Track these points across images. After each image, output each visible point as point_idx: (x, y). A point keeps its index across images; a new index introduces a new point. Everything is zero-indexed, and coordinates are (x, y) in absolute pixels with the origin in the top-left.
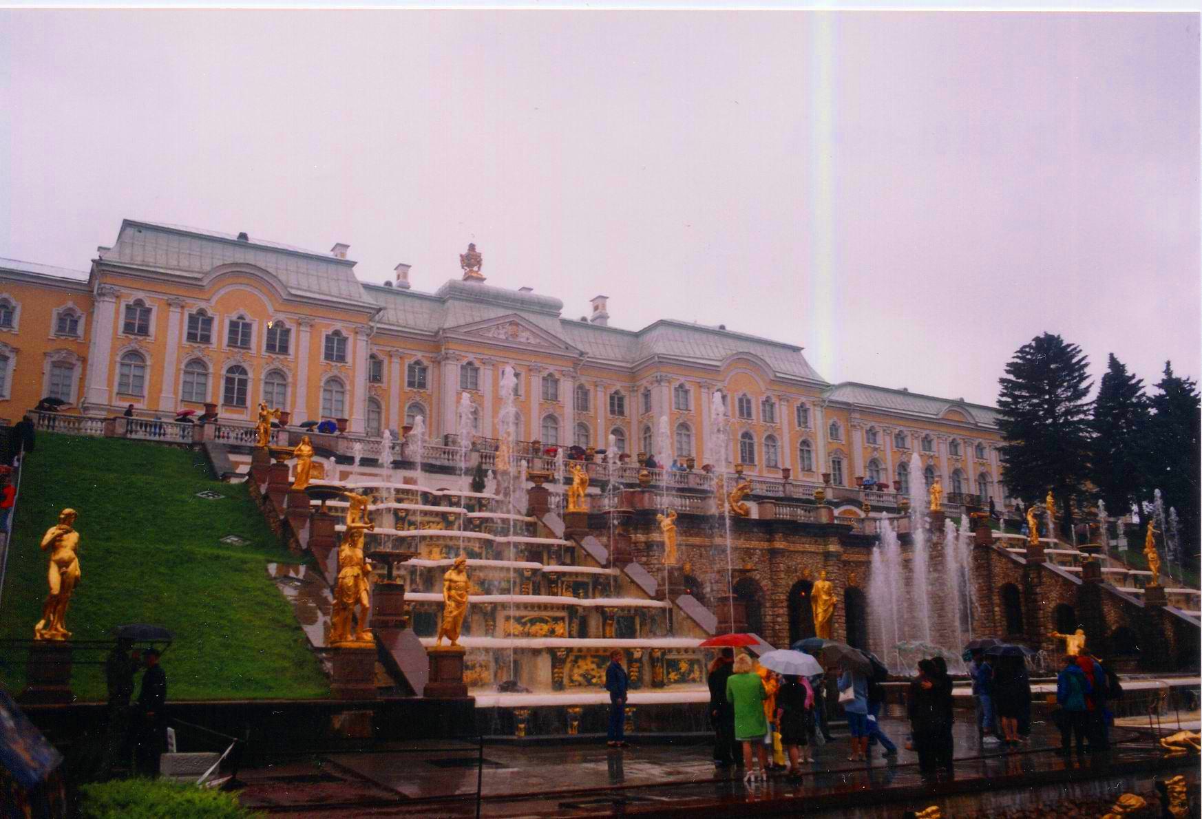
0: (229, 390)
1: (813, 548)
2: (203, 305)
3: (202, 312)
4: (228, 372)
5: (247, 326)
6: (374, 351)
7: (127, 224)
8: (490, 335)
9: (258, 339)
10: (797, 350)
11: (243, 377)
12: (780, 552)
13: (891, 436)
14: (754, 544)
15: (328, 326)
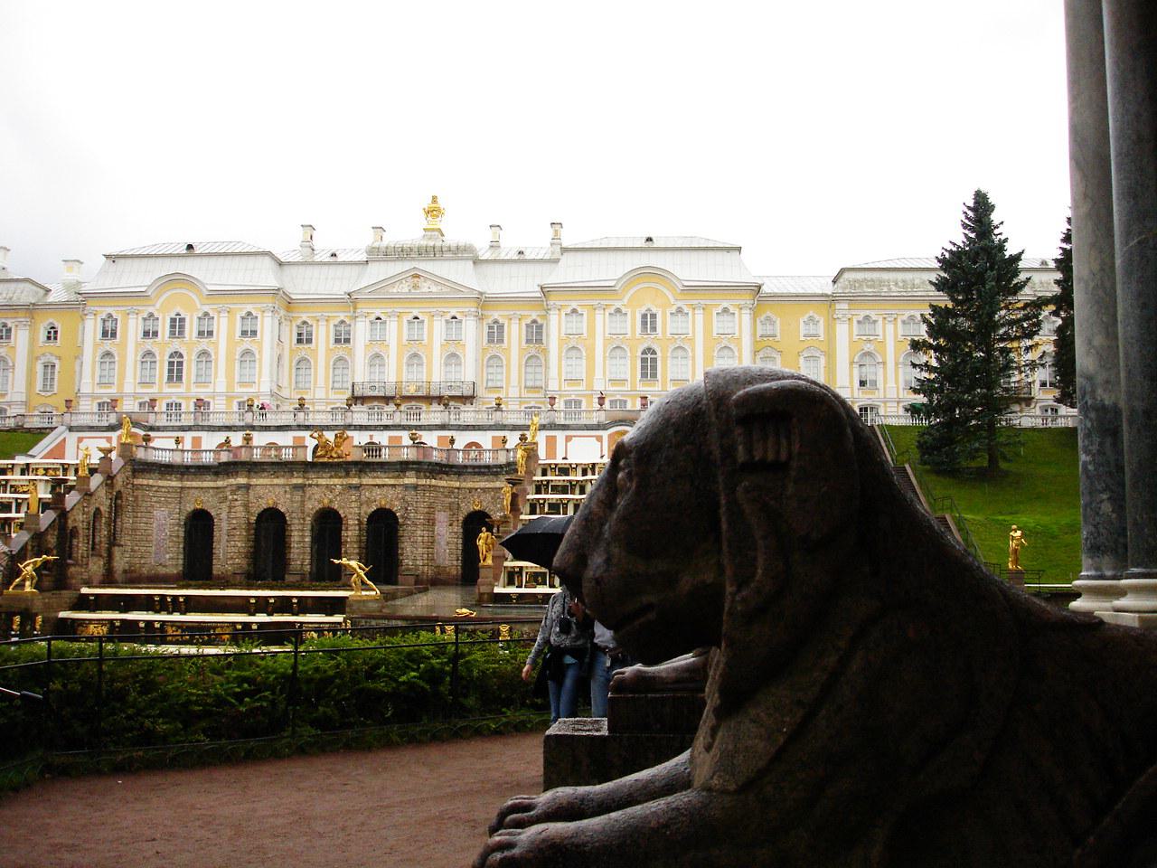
0: (171, 371)
1: (392, 482)
2: (151, 309)
3: (151, 315)
4: (170, 357)
5: (182, 320)
6: (304, 319)
7: (107, 257)
8: (395, 291)
9: (191, 328)
10: (739, 249)
11: (179, 360)
12: (357, 487)
13: (896, 325)
14: (332, 481)
15: (241, 309)
